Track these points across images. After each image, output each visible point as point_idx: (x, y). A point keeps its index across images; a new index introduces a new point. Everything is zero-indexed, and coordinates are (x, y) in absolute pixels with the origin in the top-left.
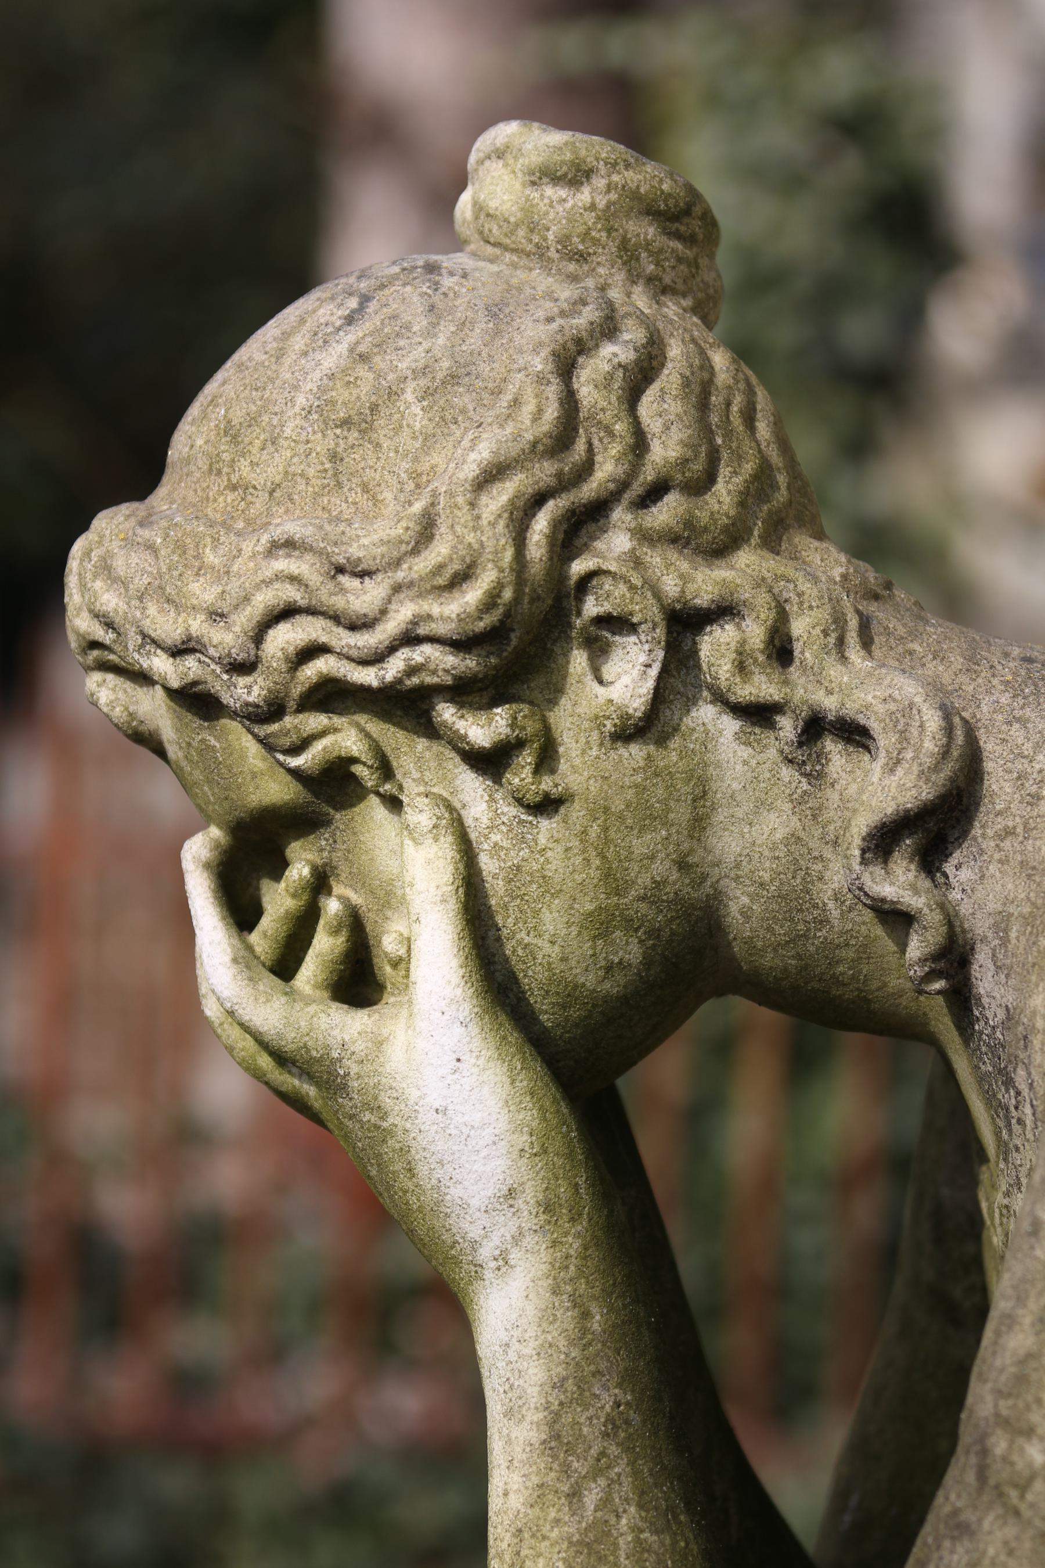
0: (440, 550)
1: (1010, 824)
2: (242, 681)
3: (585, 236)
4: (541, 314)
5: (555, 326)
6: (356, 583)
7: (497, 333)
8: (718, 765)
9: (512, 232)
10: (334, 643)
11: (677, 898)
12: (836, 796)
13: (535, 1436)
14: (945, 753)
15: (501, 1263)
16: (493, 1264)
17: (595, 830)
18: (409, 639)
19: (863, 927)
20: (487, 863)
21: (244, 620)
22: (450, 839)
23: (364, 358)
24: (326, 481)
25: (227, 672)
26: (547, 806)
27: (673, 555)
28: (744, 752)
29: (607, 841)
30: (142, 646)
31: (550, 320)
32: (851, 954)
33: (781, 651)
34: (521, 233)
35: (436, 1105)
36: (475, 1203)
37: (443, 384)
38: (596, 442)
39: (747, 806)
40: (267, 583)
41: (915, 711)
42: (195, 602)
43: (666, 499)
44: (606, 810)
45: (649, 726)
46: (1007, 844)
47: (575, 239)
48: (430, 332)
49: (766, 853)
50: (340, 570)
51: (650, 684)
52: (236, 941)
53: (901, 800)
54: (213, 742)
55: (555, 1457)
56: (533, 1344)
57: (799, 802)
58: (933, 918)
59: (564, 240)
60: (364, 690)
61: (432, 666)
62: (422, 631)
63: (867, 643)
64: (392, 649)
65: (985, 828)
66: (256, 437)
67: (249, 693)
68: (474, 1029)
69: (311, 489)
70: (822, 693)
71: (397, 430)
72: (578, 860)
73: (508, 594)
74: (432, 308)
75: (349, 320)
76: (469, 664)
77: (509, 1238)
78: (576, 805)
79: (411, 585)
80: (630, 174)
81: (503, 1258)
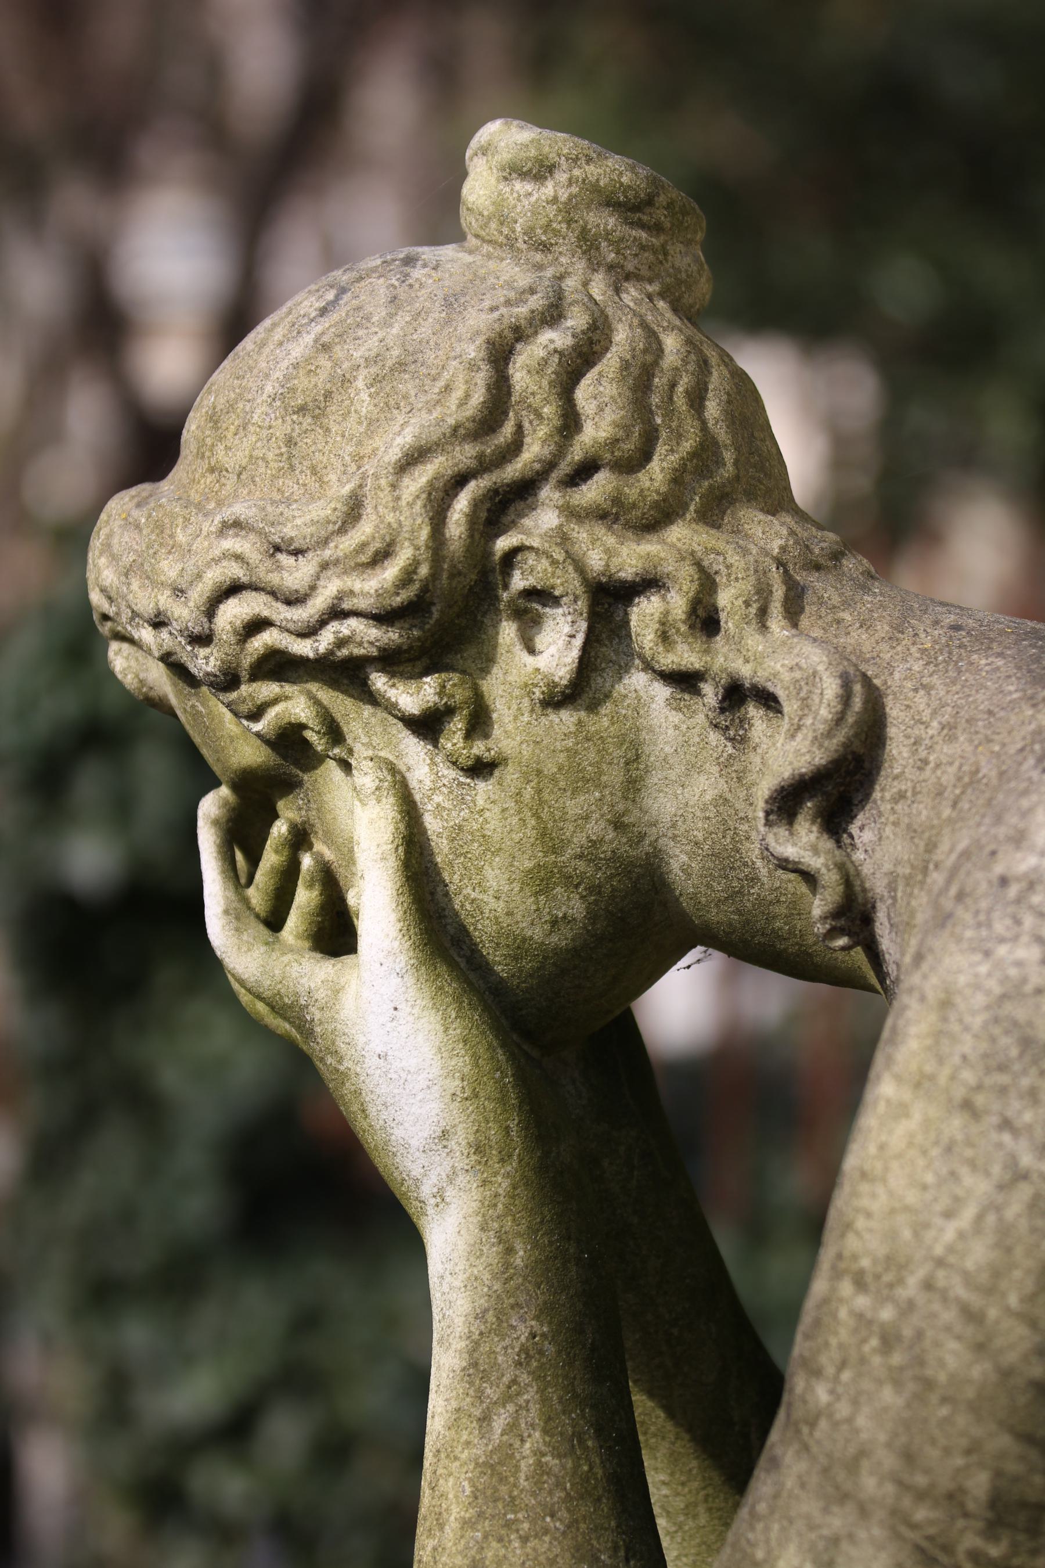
0: (365, 530)
1: (903, 787)
2: (203, 652)
3: (547, 227)
4: (487, 304)
5: (496, 315)
6: (291, 560)
7: (448, 322)
8: (651, 730)
9: (486, 225)
10: (275, 617)
11: (614, 856)
12: (757, 760)
14: (839, 720)
15: (439, 1200)
16: (433, 1201)
17: (529, 792)
18: (336, 613)
19: (790, 885)
20: (432, 824)
21: (199, 594)
22: (392, 800)
23: (326, 348)
24: (281, 465)
25: (190, 643)
26: (480, 769)
27: (600, 530)
28: (675, 717)
29: (541, 802)
30: (132, 619)
31: (493, 309)
32: (782, 910)
33: (706, 621)
34: (493, 225)
35: (378, 1051)
36: (414, 1143)
37: (394, 370)
38: (526, 425)
39: (680, 769)
40: (216, 561)
41: (817, 680)
42: (163, 578)
43: (596, 477)
44: (539, 772)
45: (580, 691)
46: (899, 807)
47: (539, 231)
48: (386, 324)
49: (698, 813)
50: (277, 549)
51: (575, 653)
52: (231, 894)
53: (796, 764)
54: (201, 708)
55: (471, 1383)
56: (462, 1277)
57: (725, 765)
58: (830, 878)
59: (529, 232)
61: (358, 639)
62: (346, 606)
63: (793, 611)
64: (323, 623)
65: (884, 791)
66: (230, 423)
67: (207, 663)
68: (410, 980)
69: (269, 472)
70: (741, 661)
71: (345, 416)
72: (515, 820)
73: (424, 570)
74: (394, 299)
75: (323, 312)
76: (392, 636)
77: (444, 1176)
78: (510, 768)
79: (337, 562)
80: (591, 169)
81: (440, 1194)
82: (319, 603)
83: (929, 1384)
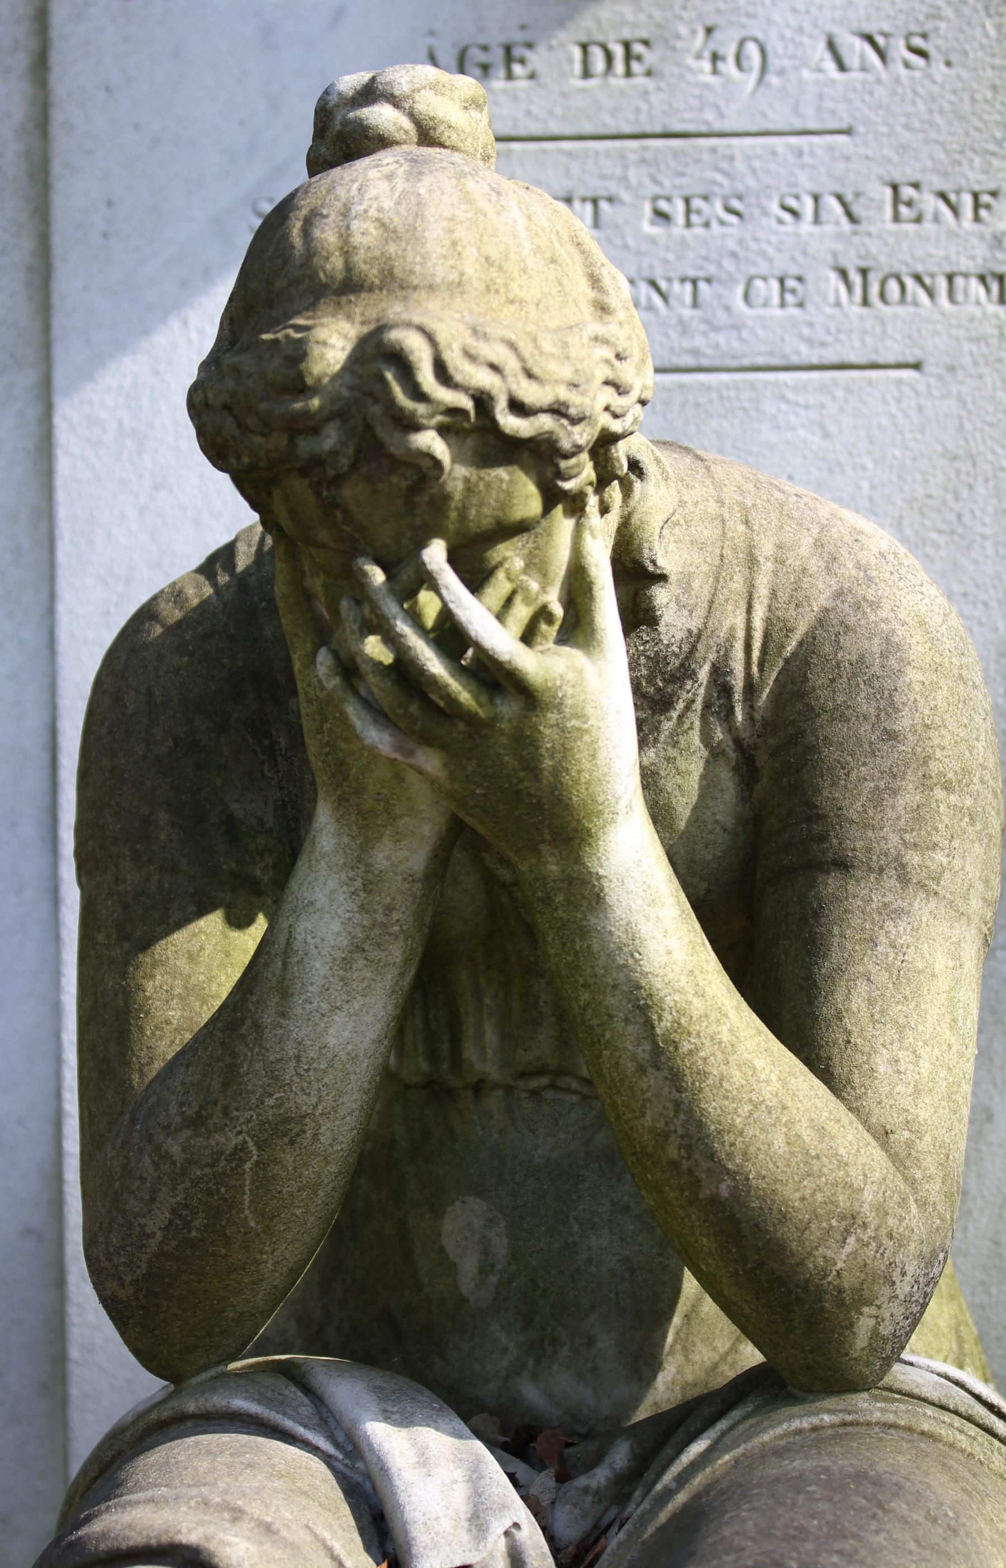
16: (624, 811)
42: (557, 377)
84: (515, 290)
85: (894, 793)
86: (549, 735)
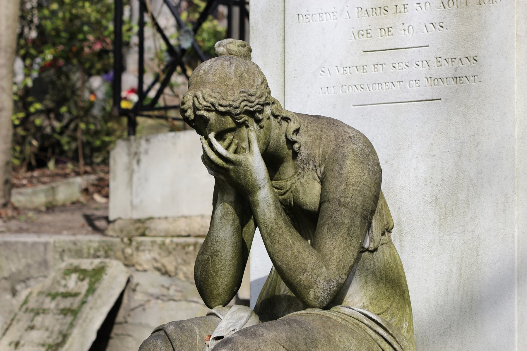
13: (274, 208)
18: (257, 104)
21: (239, 102)
59: (244, 54)
60: (251, 111)
82: (256, 102)
83: (365, 196)
84: (227, 83)
85: (340, 186)
86: (241, 172)
